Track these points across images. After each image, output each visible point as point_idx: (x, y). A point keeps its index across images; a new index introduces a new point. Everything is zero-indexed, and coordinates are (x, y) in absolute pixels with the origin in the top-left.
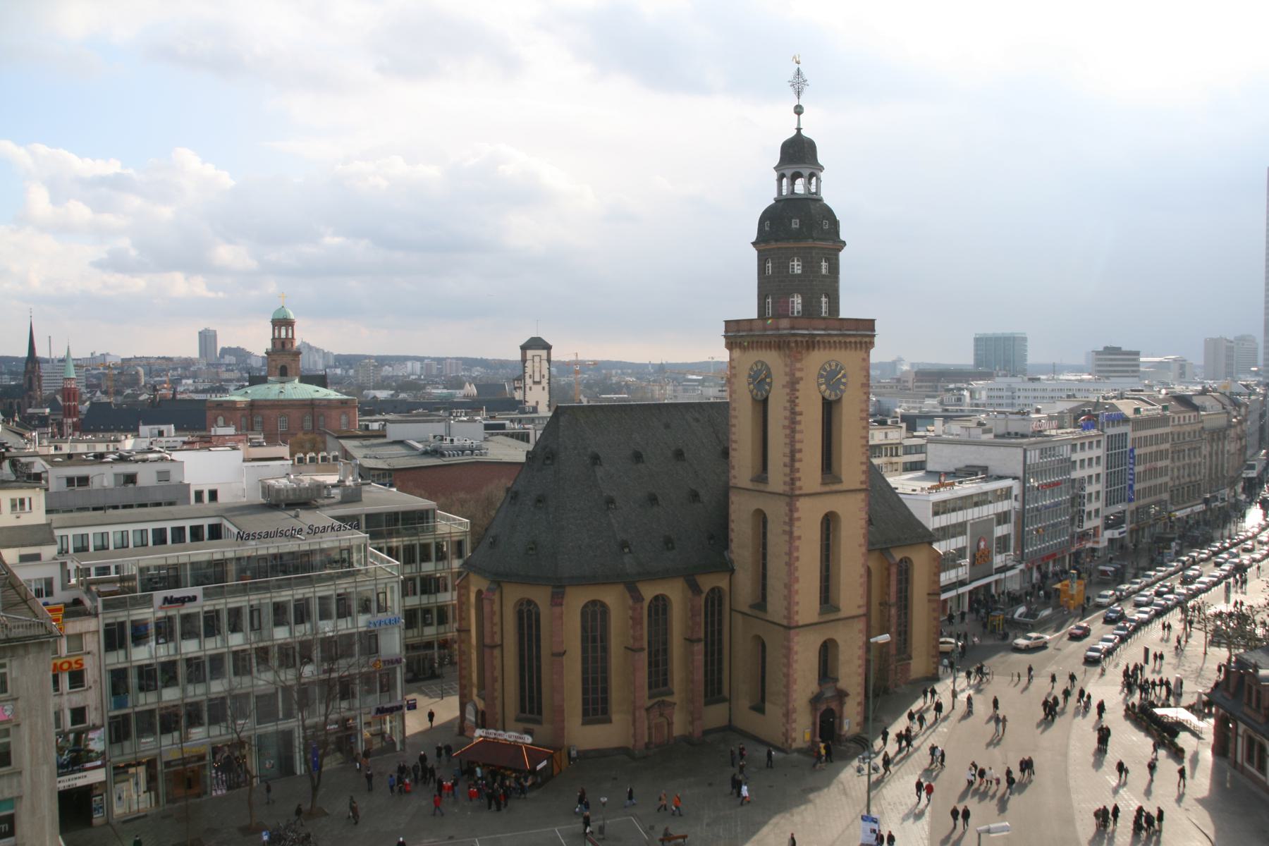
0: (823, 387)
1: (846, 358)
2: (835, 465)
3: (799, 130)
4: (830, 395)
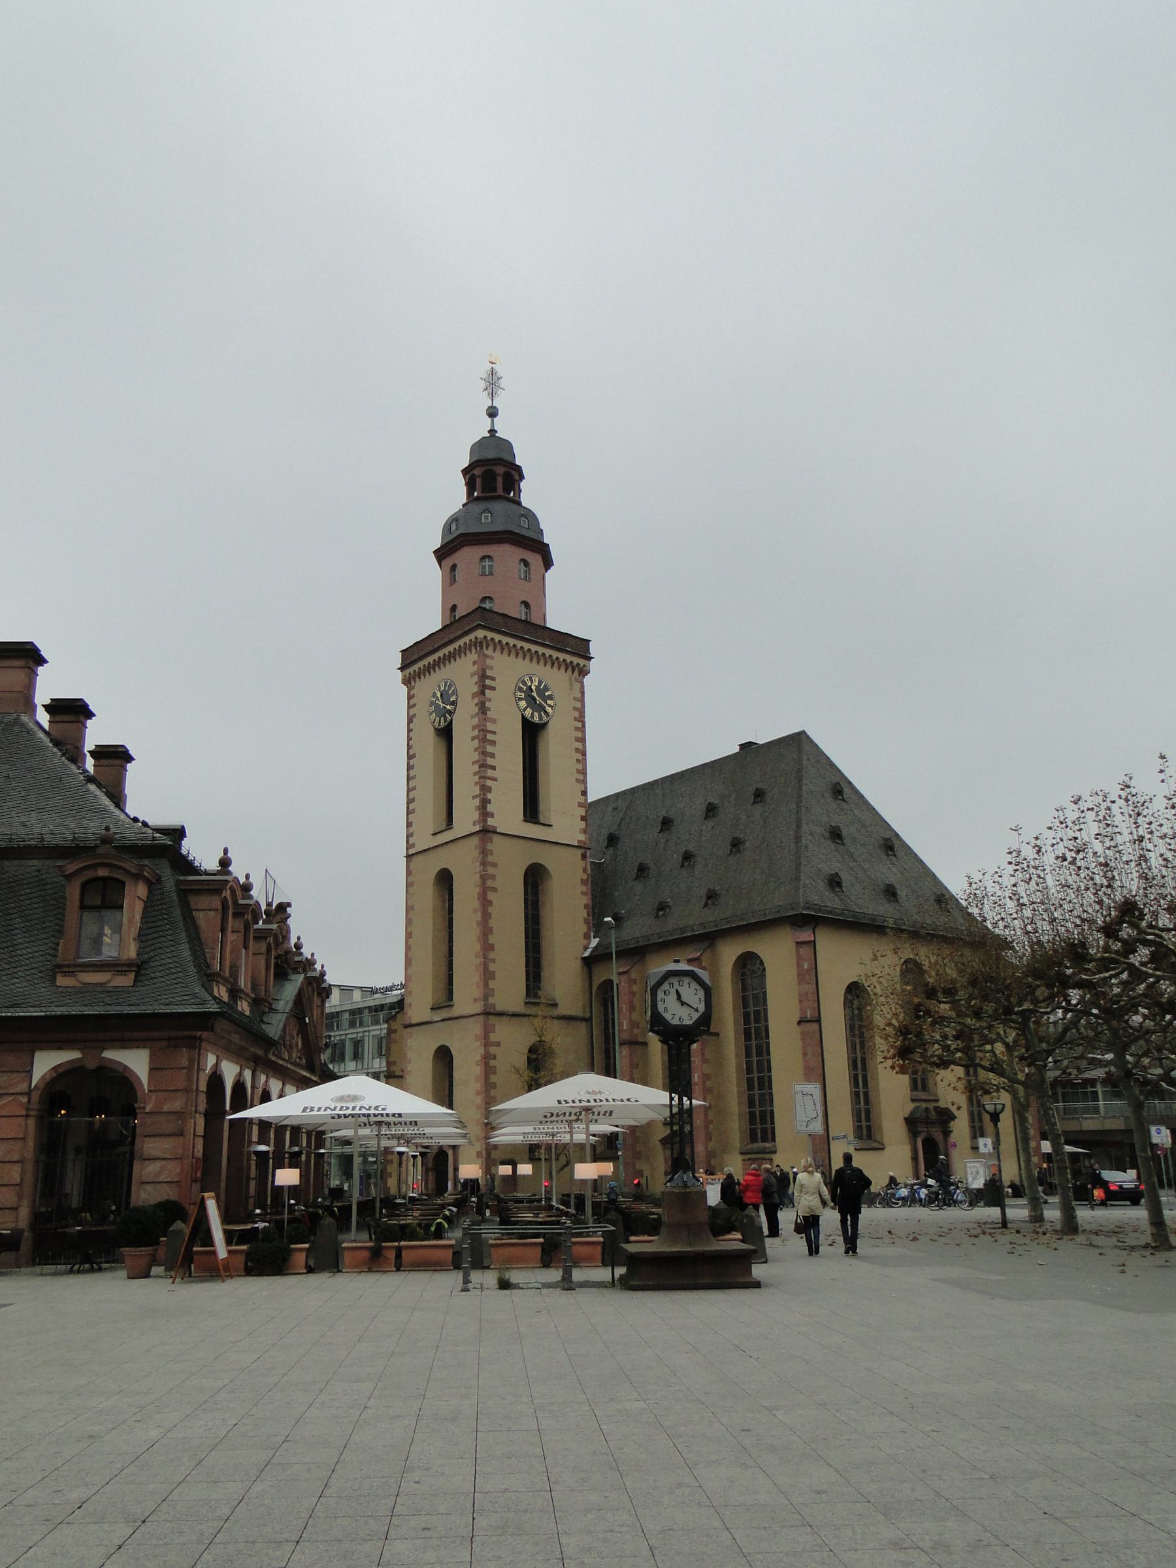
0: (523, 704)
1: (556, 680)
2: (541, 807)
3: (492, 432)
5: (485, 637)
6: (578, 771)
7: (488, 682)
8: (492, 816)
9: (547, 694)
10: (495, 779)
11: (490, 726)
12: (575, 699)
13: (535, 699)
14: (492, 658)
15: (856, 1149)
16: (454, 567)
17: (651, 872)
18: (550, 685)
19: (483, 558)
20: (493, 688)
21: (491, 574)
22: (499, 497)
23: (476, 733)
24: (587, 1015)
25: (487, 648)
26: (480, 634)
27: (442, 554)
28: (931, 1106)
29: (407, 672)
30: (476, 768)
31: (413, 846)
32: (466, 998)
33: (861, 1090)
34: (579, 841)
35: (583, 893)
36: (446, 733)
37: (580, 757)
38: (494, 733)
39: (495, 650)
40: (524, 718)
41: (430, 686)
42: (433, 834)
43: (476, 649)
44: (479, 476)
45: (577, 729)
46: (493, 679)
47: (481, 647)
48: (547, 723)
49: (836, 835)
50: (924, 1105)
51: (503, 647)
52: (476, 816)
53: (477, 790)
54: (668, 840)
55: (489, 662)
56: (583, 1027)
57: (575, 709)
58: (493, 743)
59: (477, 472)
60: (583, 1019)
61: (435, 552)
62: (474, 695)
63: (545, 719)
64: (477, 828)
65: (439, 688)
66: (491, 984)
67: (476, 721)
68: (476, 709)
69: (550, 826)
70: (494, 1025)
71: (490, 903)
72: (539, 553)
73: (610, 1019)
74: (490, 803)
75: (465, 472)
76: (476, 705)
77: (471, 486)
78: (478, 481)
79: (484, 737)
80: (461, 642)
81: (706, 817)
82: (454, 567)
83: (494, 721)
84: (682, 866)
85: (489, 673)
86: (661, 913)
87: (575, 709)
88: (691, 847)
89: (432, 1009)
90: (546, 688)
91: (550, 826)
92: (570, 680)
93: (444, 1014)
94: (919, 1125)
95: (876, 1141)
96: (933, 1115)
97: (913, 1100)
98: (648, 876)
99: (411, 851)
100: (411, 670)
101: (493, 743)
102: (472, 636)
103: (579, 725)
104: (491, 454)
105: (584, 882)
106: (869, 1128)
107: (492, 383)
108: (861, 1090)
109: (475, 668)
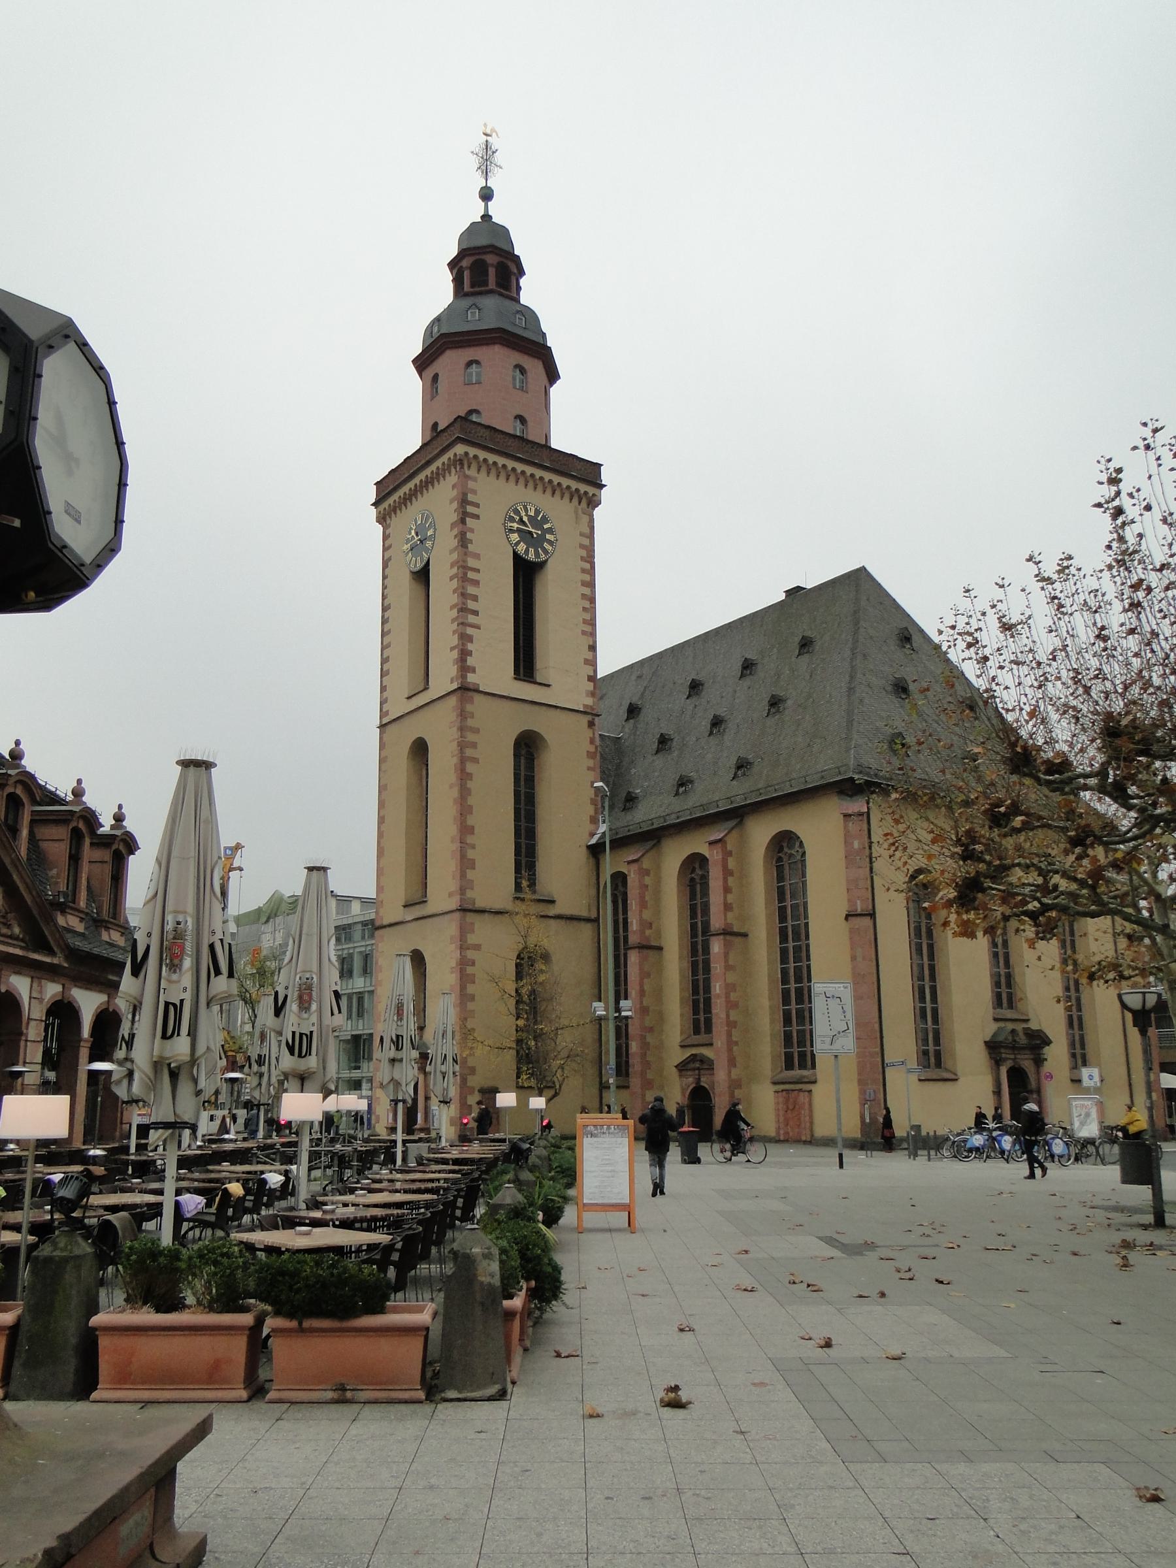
0: (515, 537)
1: (558, 511)
2: (539, 664)
3: (486, 217)
4: (527, 551)
5: (466, 454)
6: (585, 622)
7: (470, 509)
8: (473, 670)
10: (478, 627)
11: (471, 562)
12: (582, 534)
13: (530, 533)
14: (475, 480)
15: (920, 1080)
16: (435, 378)
17: (675, 743)
18: (550, 515)
19: (469, 364)
20: (477, 517)
21: (479, 383)
22: (491, 292)
23: (455, 570)
24: (594, 915)
25: (469, 467)
26: (460, 449)
27: (422, 363)
28: (1019, 1027)
29: (381, 508)
30: (454, 613)
31: (387, 713)
32: (442, 895)
33: (929, 1005)
34: (585, 706)
35: (589, 769)
36: (423, 576)
37: (587, 604)
38: (478, 571)
39: (479, 470)
41: (408, 520)
42: (409, 698)
43: (455, 468)
44: (467, 268)
45: (583, 571)
46: (477, 505)
47: (462, 464)
48: (546, 561)
49: (901, 689)
50: (1010, 1026)
51: (491, 468)
52: (453, 671)
53: (455, 640)
54: (696, 706)
55: (471, 484)
56: (587, 930)
57: (582, 546)
58: (476, 583)
59: (465, 263)
60: (588, 920)
61: (414, 361)
62: (453, 525)
63: (543, 557)
64: (455, 686)
65: (416, 523)
66: (470, 874)
67: (455, 556)
68: (455, 543)
69: (548, 686)
70: (472, 924)
71: (470, 776)
72: (539, 358)
73: (621, 920)
74: (471, 655)
75: (453, 265)
76: (456, 536)
77: (458, 281)
78: (466, 274)
79: (465, 575)
80: (438, 463)
81: (742, 676)
82: (435, 378)
83: (477, 556)
84: (711, 733)
85: (470, 497)
86: (682, 790)
87: (582, 546)
88: (722, 712)
89: (405, 906)
90: (545, 520)
91: (548, 686)
92: (576, 512)
93: (417, 912)
94: (1003, 1050)
95: (947, 1070)
96: (1022, 1040)
97: (996, 1020)
98: (670, 748)
99: (385, 721)
100: (385, 505)
101: (476, 583)
102: (450, 454)
103: (588, 566)
104: (482, 241)
105: (590, 755)
106: (938, 1054)
107: (487, 159)
108: (929, 1005)
109: (455, 493)
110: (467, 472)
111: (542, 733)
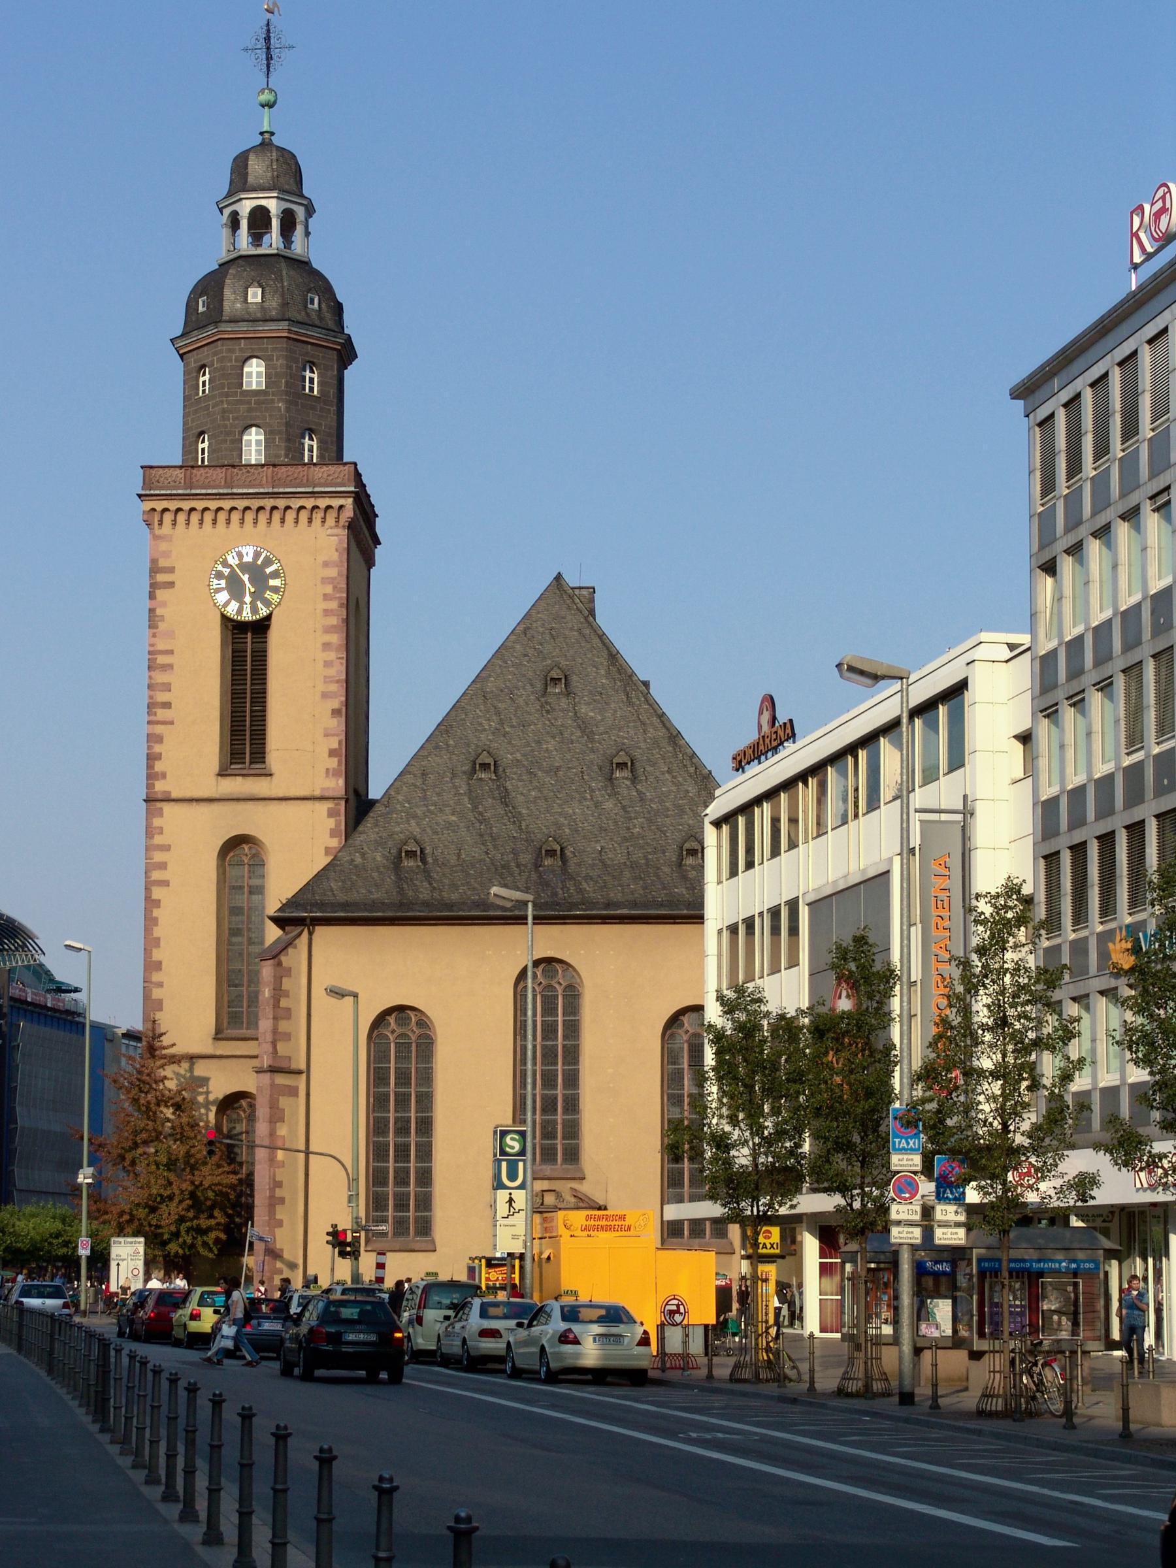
0: (223, 597)
4: (240, 611)
9: (268, 571)
40: (225, 618)
48: (268, 618)
55: (163, 546)
63: (264, 611)
85: (162, 563)
110: (157, 532)
111: (261, 838)
